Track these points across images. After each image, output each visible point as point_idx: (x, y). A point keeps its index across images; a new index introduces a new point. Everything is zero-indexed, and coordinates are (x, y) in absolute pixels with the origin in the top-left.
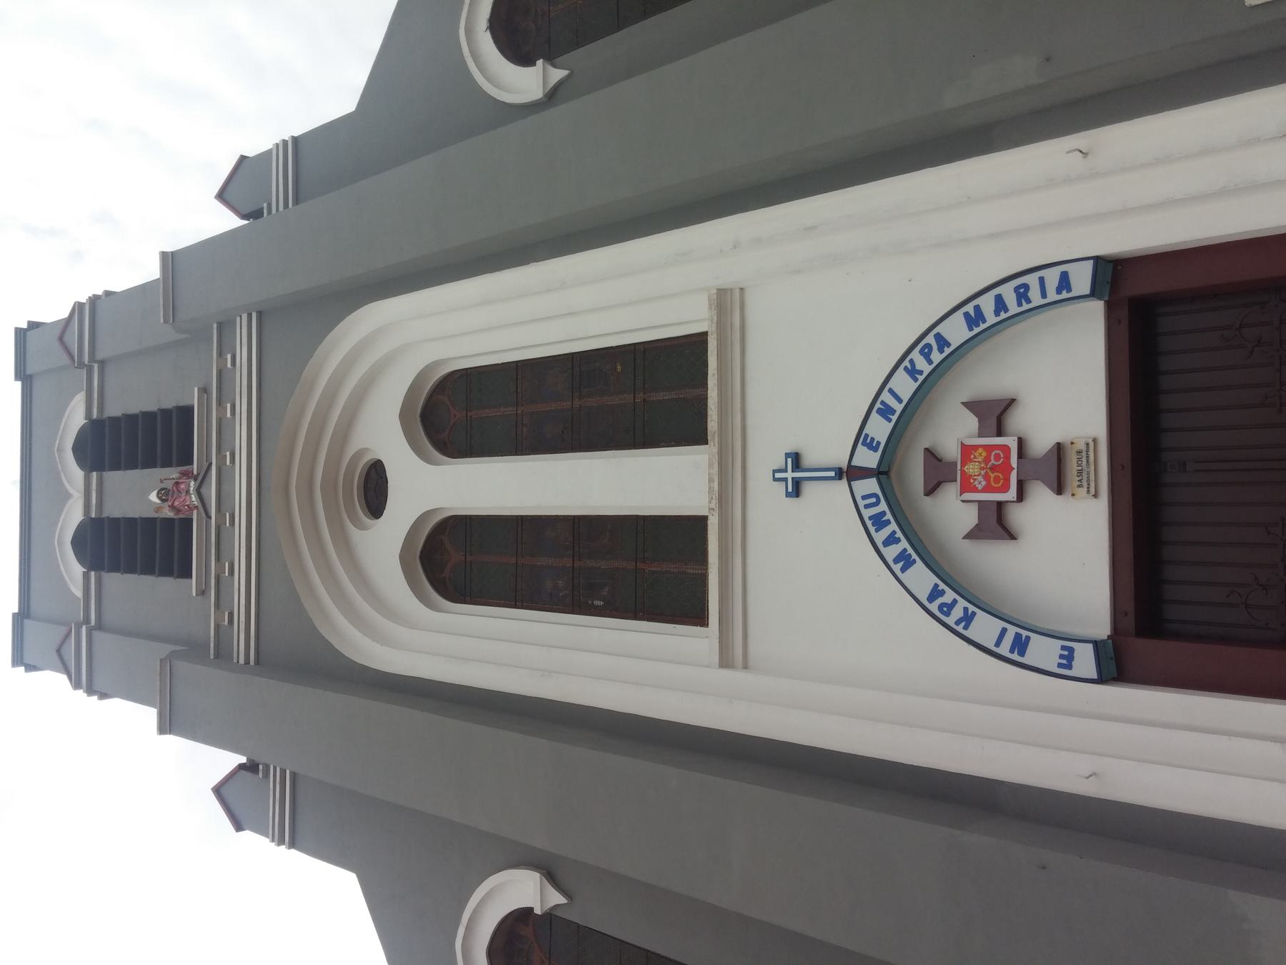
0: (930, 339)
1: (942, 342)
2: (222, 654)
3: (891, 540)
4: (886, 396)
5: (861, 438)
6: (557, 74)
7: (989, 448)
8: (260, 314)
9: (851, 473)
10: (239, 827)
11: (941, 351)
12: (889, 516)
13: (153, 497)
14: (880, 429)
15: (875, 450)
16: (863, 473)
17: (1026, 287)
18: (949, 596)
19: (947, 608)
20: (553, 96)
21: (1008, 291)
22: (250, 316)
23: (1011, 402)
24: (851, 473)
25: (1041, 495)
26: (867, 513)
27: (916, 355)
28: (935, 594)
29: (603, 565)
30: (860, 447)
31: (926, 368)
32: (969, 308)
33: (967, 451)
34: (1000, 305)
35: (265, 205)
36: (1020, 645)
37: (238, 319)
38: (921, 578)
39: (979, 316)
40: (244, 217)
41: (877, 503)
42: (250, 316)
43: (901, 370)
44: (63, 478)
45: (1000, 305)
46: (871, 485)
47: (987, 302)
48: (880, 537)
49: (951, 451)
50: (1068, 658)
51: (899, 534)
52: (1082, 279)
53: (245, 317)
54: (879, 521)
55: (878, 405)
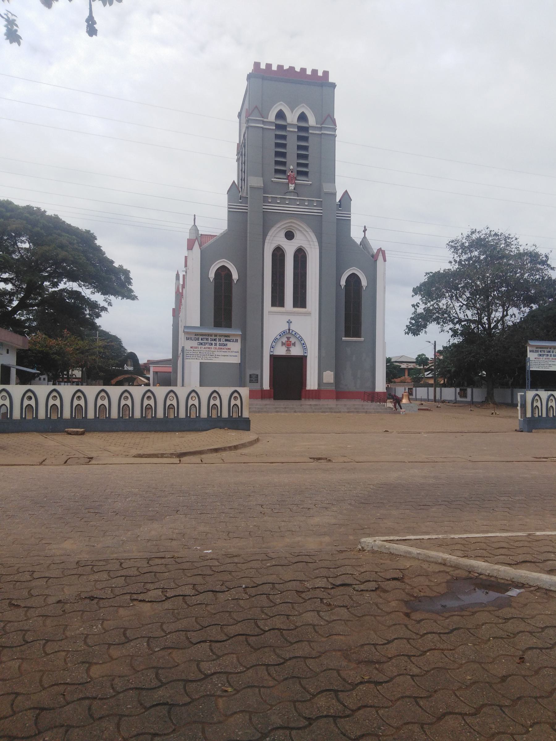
1: (302, 340)
2: (265, 199)
5: (293, 331)
8: (322, 216)
9: (289, 330)
13: (291, 167)
14: (294, 333)
16: (289, 331)
19: (276, 340)
21: (305, 347)
22: (322, 213)
23: (295, 346)
24: (289, 330)
25: (286, 349)
28: (277, 339)
29: (278, 288)
33: (291, 342)
34: (304, 347)
35: (341, 209)
36: (273, 347)
37: (322, 208)
38: (278, 337)
39: (304, 344)
40: (340, 201)
42: (322, 213)
44: (297, 108)
45: (304, 347)
46: (288, 332)
47: (305, 345)
48: (282, 332)
49: (290, 340)
50: (272, 352)
52: (305, 354)
53: (321, 211)
54: (284, 332)
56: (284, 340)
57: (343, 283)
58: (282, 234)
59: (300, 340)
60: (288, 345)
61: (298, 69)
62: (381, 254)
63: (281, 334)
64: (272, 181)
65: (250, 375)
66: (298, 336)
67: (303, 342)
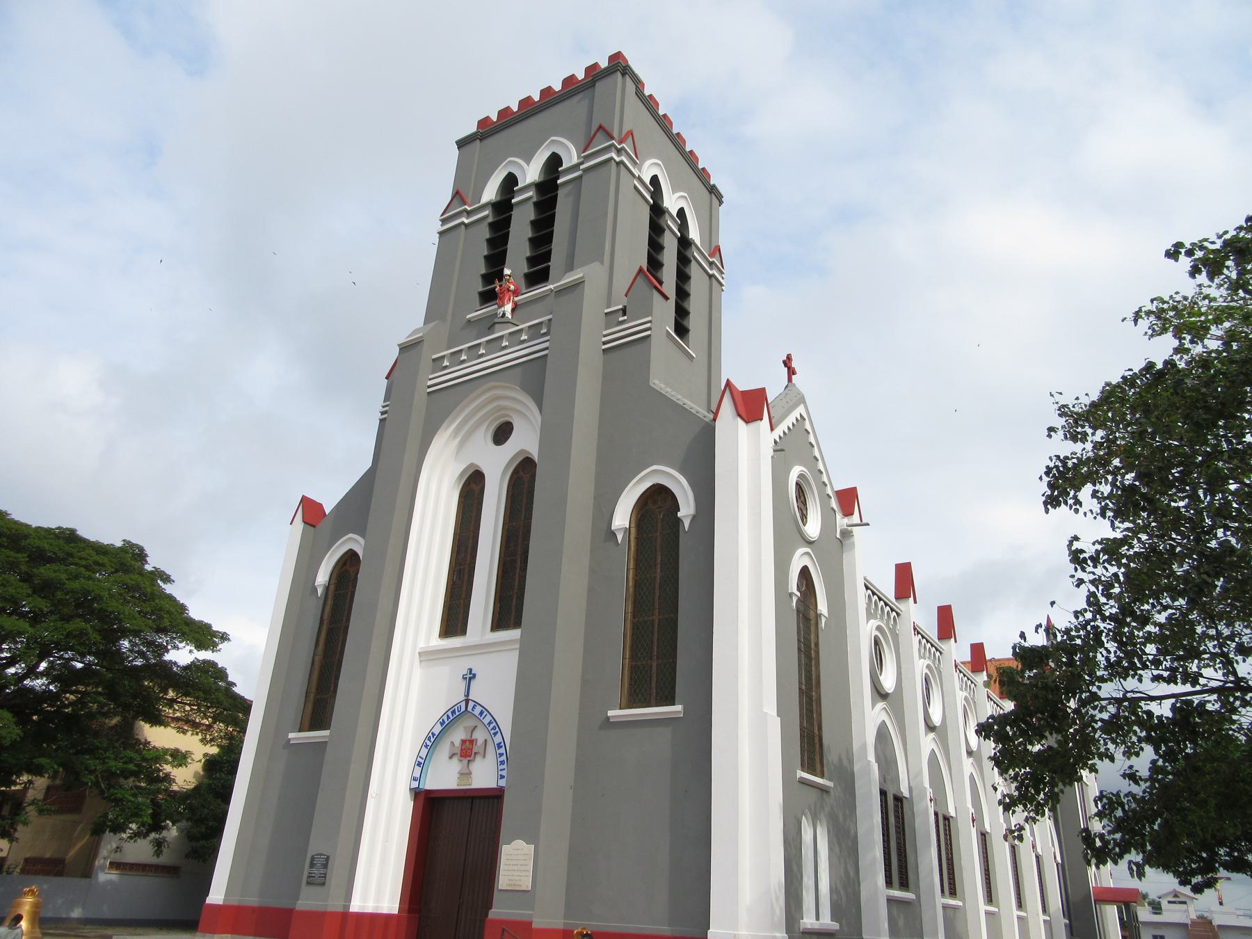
0: (497, 729)
1: (495, 734)
3: (448, 717)
4: (486, 712)
6: (620, 538)
7: (472, 749)
9: (467, 701)
10: (387, 378)
11: (494, 734)
12: (455, 716)
15: (472, 710)
17: (503, 764)
18: (432, 740)
19: (429, 739)
20: (613, 534)
24: (467, 701)
26: (456, 707)
27: (494, 724)
28: (433, 734)
30: (474, 703)
31: (490, 729)
32: (502, 744)
34: (501, 755)
38: (437, 730)
41: (458, 711)
43: (492, 719)
45: (501, 755)
46: (463, 709)
47: (502, 751)
48: (449, 713)
51: (449, 720)
54: (454, 712)
55: (484, 710)
56: (458, 735)
57: (622, 518)
58: (483, 437)
59: (493, 732)
60: (467, 751)
61: (557, 87)
62: (727, 399)
63: (446, 720)
64: (469, 321)
65: (313, 858)
66: (486, 721)
67: (498, 739)
